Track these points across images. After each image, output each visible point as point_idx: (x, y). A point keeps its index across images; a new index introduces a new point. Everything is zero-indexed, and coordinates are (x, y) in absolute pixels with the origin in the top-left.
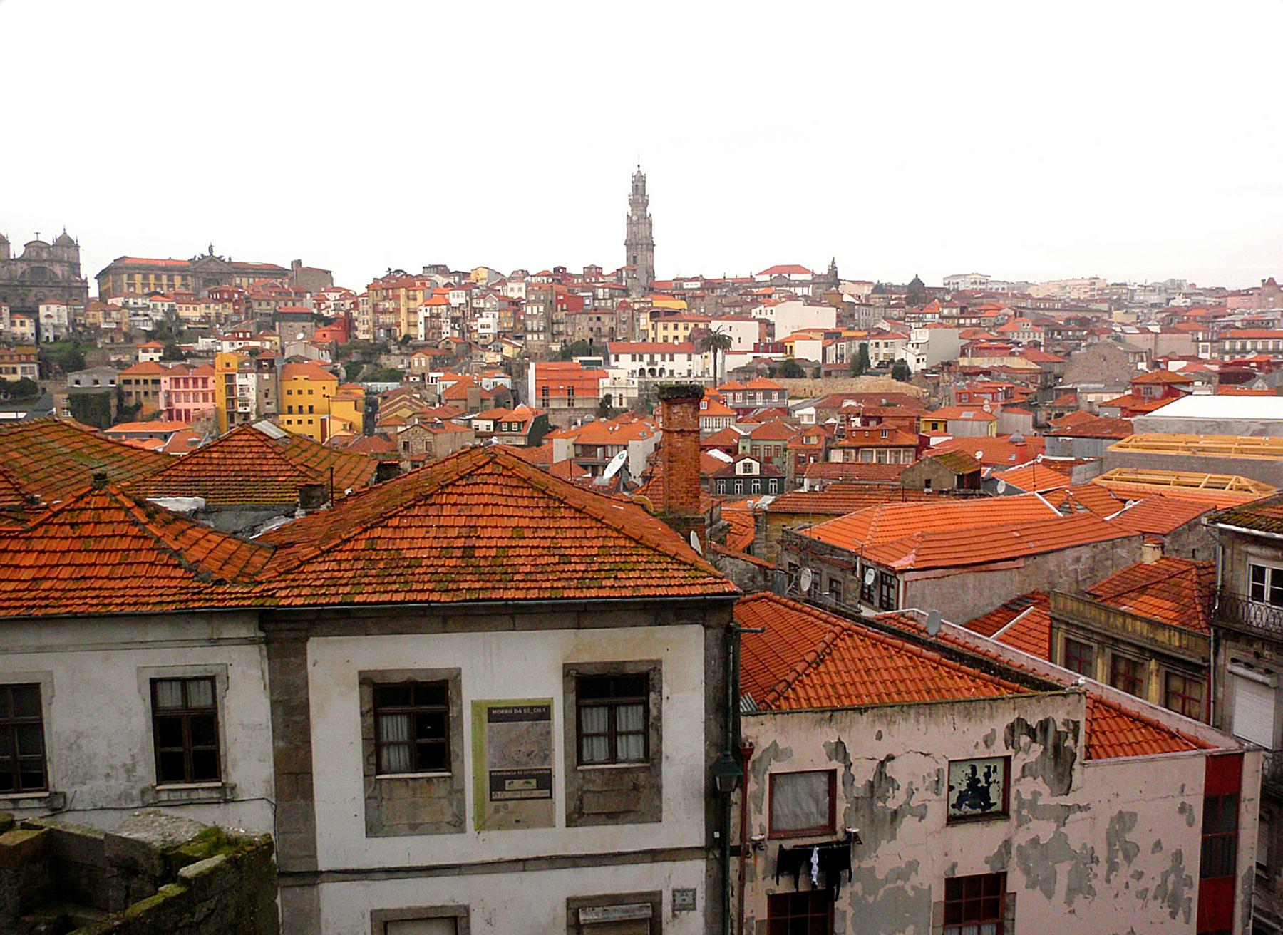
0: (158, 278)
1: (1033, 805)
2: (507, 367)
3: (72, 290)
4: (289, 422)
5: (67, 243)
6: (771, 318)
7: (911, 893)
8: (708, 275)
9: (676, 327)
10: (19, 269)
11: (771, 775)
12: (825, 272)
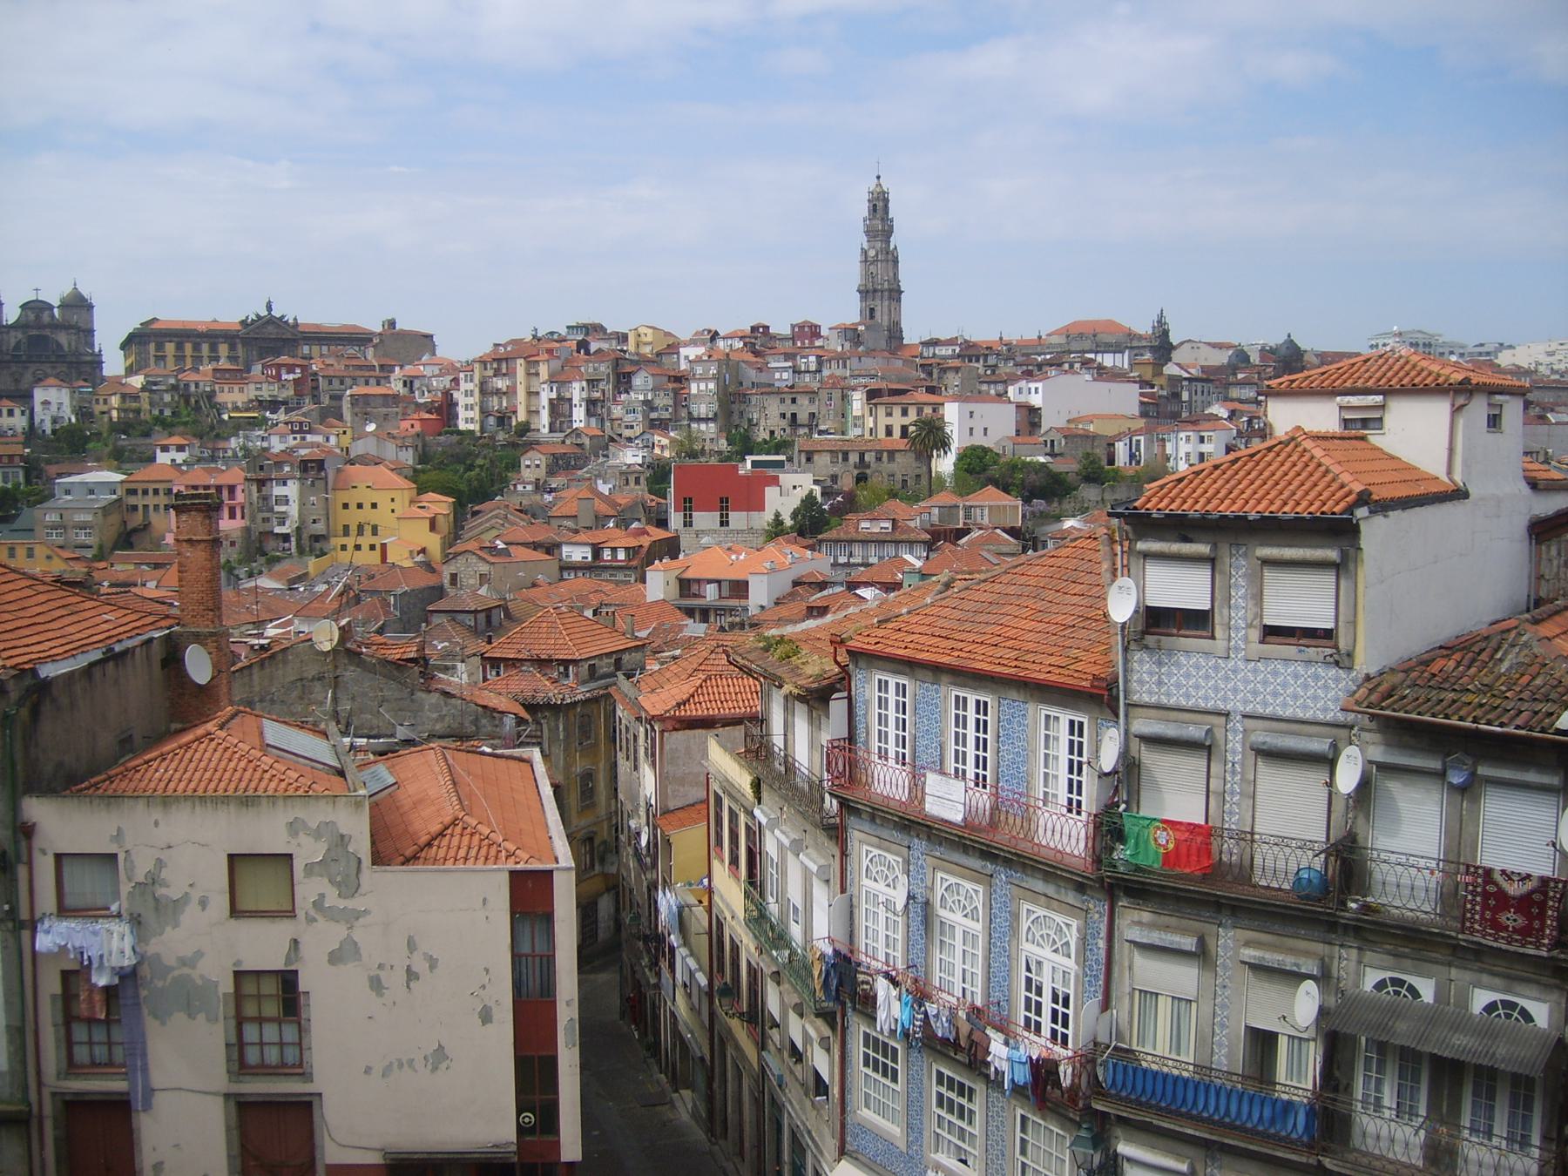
0: (197, 347)
1: (318, 905)
3: (81, 365)
4: (344, 548)
5: (78, 304)
6: (1036, 400)
7: (199, 982)
9: (905, 413)
10: (13, 338)
11: (59, 857)
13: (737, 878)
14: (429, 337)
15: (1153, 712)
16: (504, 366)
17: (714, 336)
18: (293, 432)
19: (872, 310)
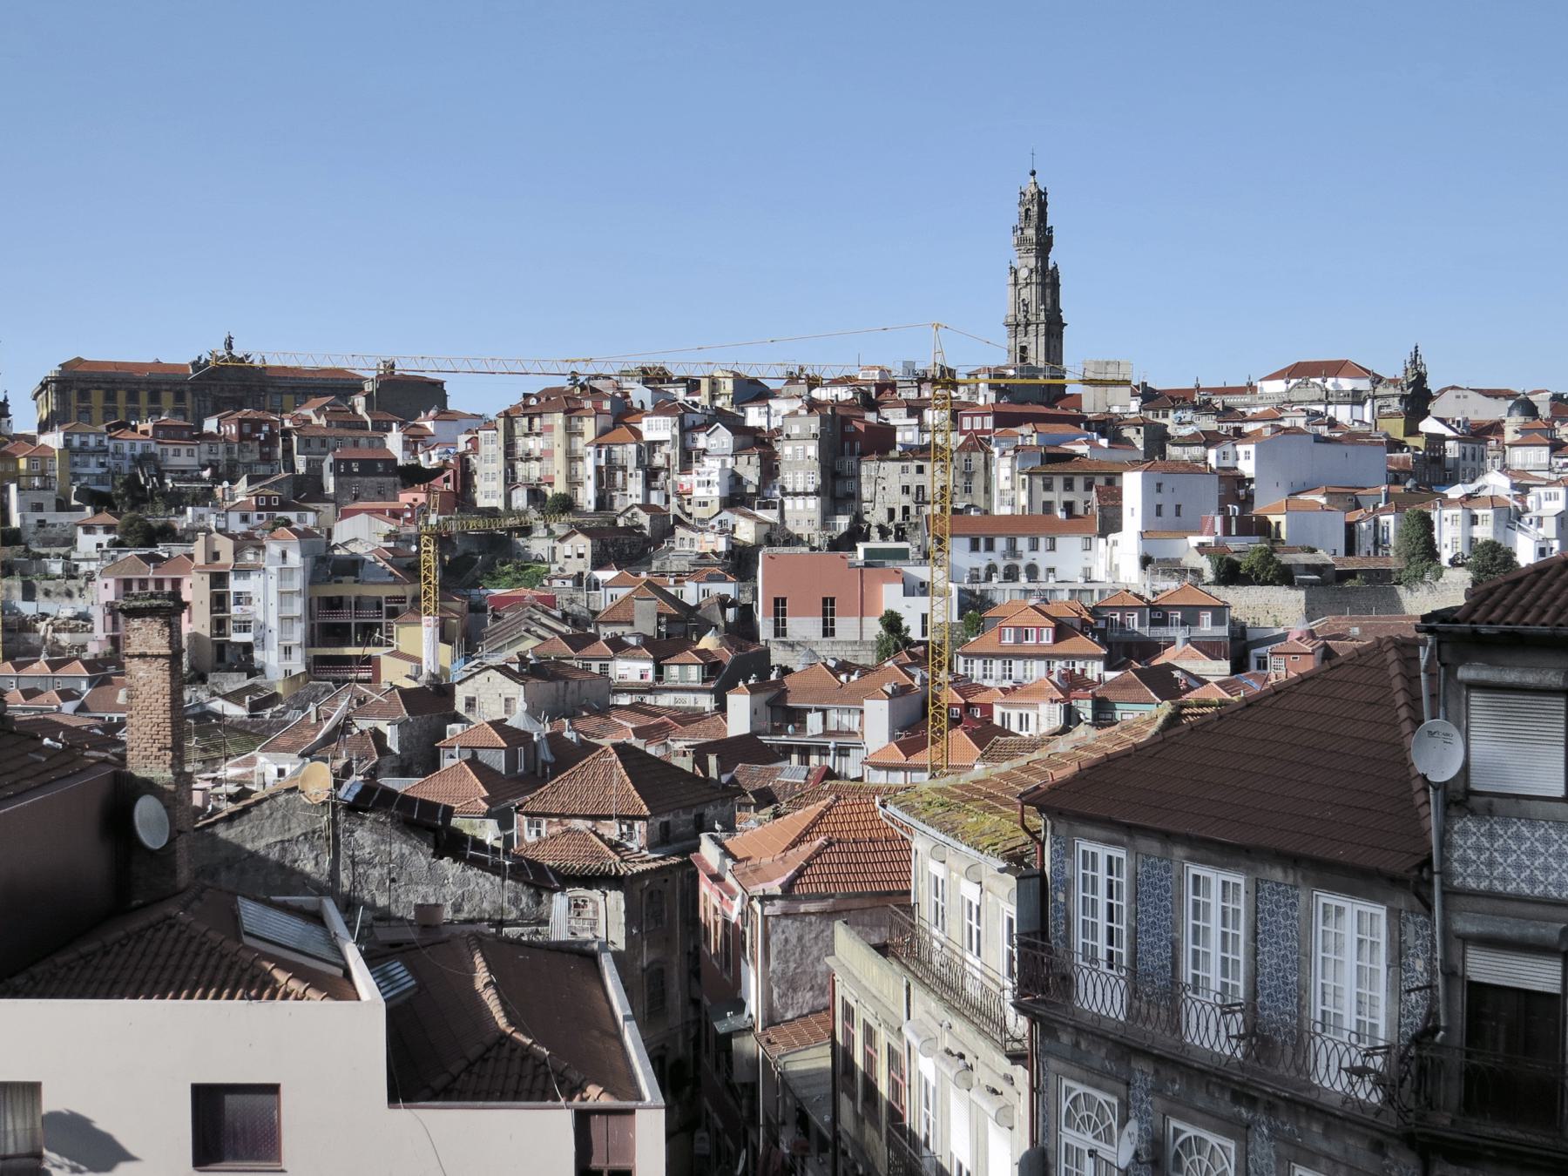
0: (133, 396)
2: (740, 561)
6: (1247, 467)
8: (1157, 384)
9: (1069, 486)
12: (1400, 375)
13: (876, 1124)
14: (442, 383)
15: (1484, 904)
16: (537, 421)
17: (813, 383)
18: (259, 508)
19: (1024, 349)
